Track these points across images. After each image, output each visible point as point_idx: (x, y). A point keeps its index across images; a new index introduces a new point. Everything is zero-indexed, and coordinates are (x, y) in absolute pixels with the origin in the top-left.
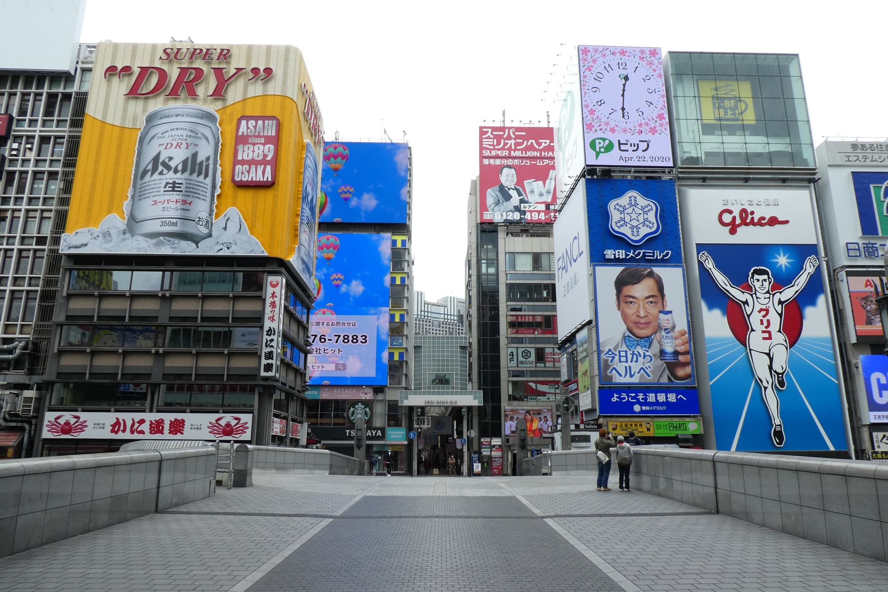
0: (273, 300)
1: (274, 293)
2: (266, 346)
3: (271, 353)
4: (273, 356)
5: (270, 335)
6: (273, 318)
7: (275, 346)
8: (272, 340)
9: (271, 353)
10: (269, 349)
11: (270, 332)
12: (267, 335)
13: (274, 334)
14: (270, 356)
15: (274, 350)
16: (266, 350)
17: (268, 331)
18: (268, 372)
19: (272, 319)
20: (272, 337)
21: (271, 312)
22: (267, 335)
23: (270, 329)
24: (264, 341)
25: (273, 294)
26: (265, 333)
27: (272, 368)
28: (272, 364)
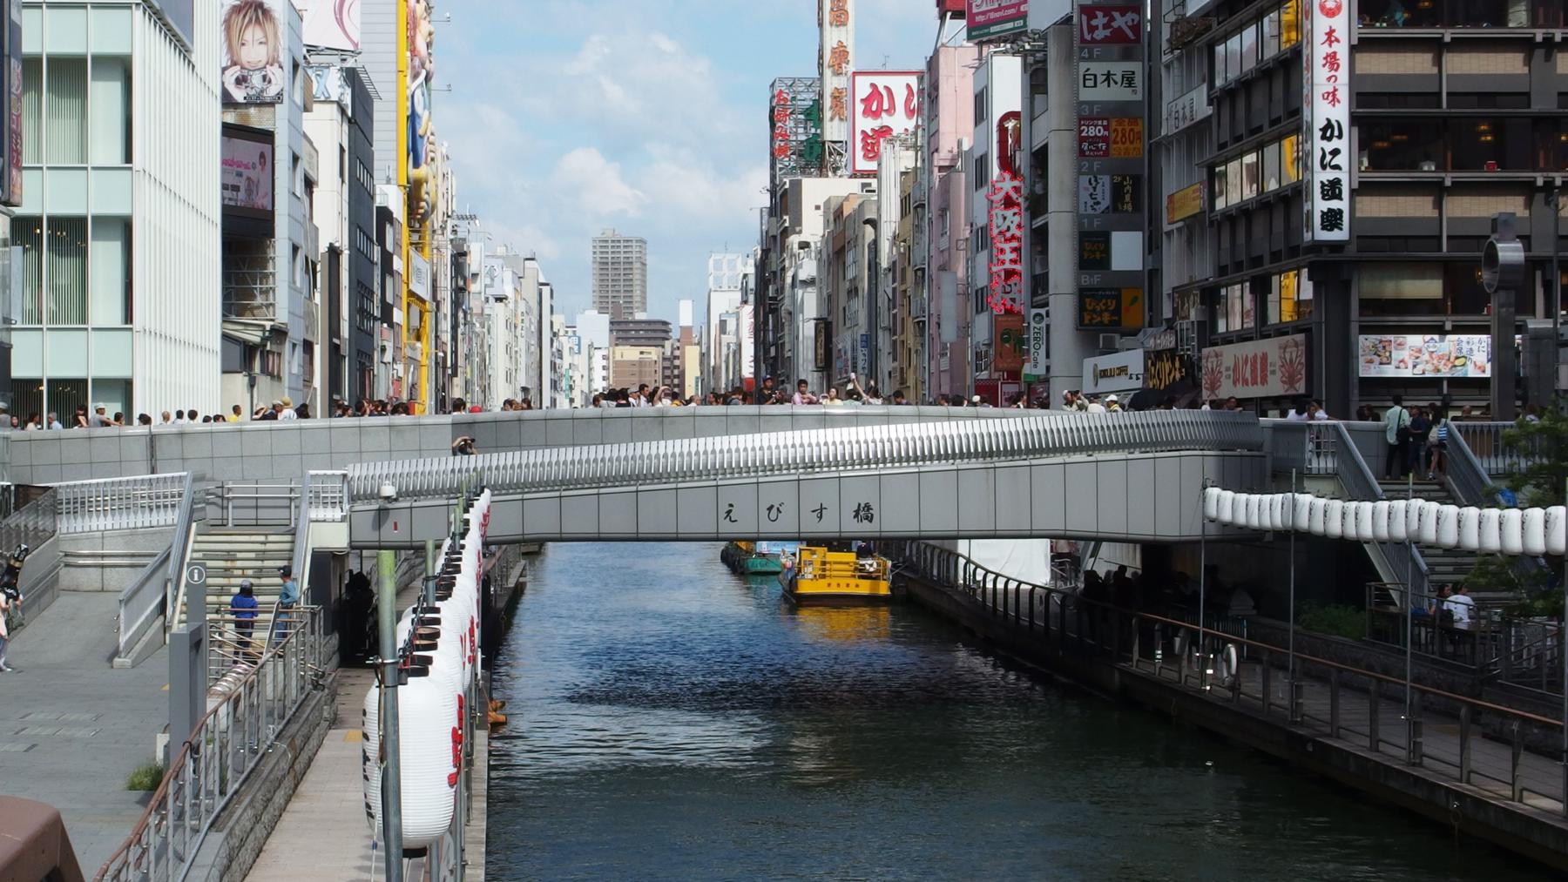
0: (1330, 51)
1: (1330, 33)
2: (1324, 167)
3: (1335, 183)
4: (1340, 191)
5: (1329, 139)
6: (1334, 95)
7: (1345, 166)
8: (1335, 152)
9: (1335, 183)
10: (1330, 175)
11: (1329, 130)
12: (1324, 137)
13: (1340, 136)
14: (1334, 192)
15: (1343, 176)
16: (1322, 176)
17: (1324, 130)
18: (1331, 230)
19: (1332, 97)
20: (1335, 144)
21: (1329, 79)
22: (1324, 137)
23: (1329, 125)
24: (1318, 155)
25: (1330, 33)
26: (1317, 134)
27: (1341, 217)
28: (1340, 212)
